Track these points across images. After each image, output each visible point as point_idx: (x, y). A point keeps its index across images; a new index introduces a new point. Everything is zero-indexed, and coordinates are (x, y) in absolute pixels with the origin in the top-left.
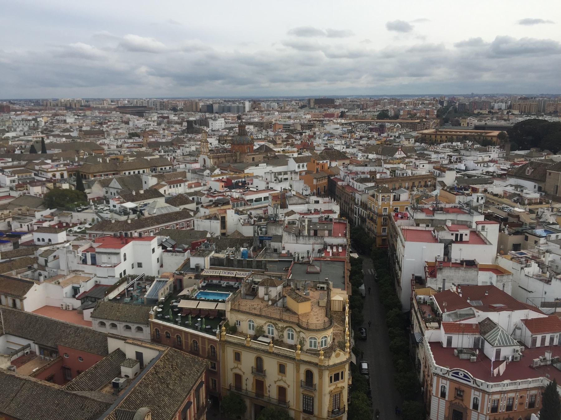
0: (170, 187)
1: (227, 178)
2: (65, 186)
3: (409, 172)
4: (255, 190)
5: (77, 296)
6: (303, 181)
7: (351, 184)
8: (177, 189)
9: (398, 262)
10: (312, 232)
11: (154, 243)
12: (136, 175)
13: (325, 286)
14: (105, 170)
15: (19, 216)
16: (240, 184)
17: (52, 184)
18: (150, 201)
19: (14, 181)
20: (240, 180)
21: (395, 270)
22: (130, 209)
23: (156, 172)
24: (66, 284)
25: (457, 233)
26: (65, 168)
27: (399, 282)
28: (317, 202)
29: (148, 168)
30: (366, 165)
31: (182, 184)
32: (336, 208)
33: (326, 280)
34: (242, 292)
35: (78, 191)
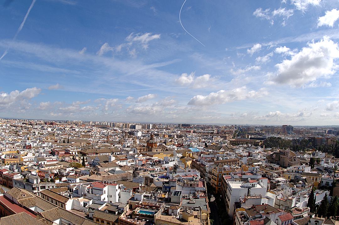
0: (121, 162)
3: (228, 158)
5: (86, 207)
7: (203, 163)
9: (228, 198)
10: (189, 185)
11: (117, 187)
13: (199, 209)
21: (226, 201)
24: (82, 201)
25: (252, 183)
26: (76, 150)
27: (228, 206)
30: (209, 155)
32: (199, 174)
33: (199, 206)
34: (161, 212)
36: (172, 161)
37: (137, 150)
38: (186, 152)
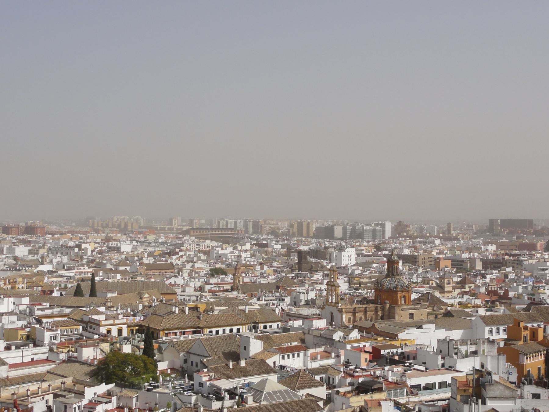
0: (283, 358)
1: (373, 348)
2: (127, 349)
4: (423, 368)
6: (503, 358)
8: (293, 362)
12: (229, 336)
14: (182, 325)
15: (64, 393)
16: (396, 358)
17: (108, 344)
18: (255, 380)
19: (55, 338)
20: (395, 350)
22: (226, 391)
23: (256, 332)
26: (125, 321)
28: (536, 396)
29: (245, 324)
31: (302, 354)
35: (145, 357)
36: (466, 356)
37: (339, 315)
38: (522, 324)
